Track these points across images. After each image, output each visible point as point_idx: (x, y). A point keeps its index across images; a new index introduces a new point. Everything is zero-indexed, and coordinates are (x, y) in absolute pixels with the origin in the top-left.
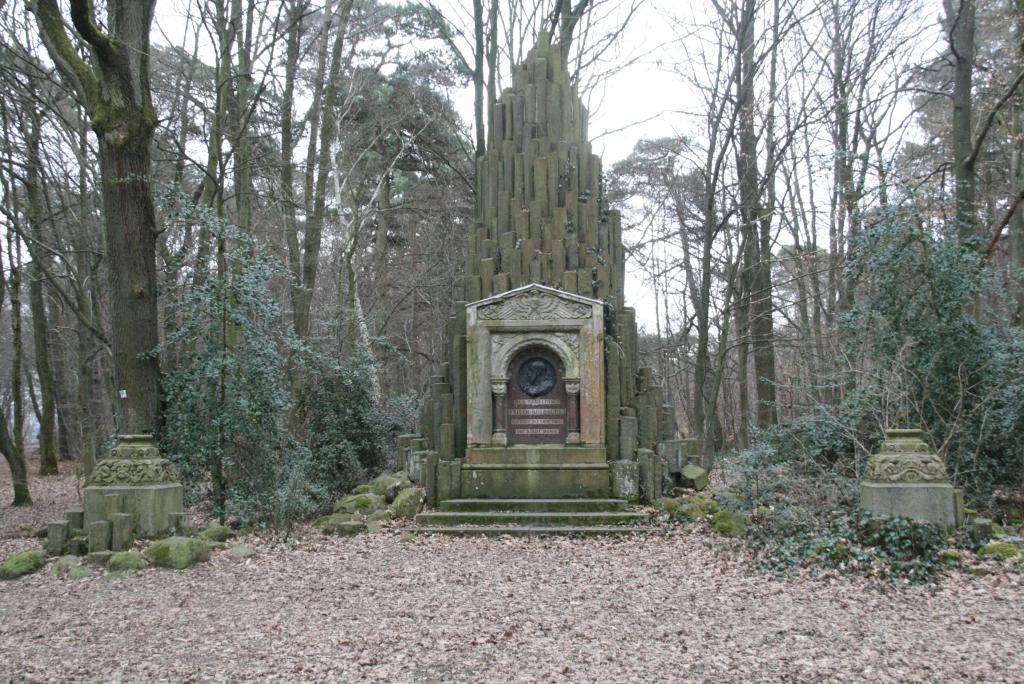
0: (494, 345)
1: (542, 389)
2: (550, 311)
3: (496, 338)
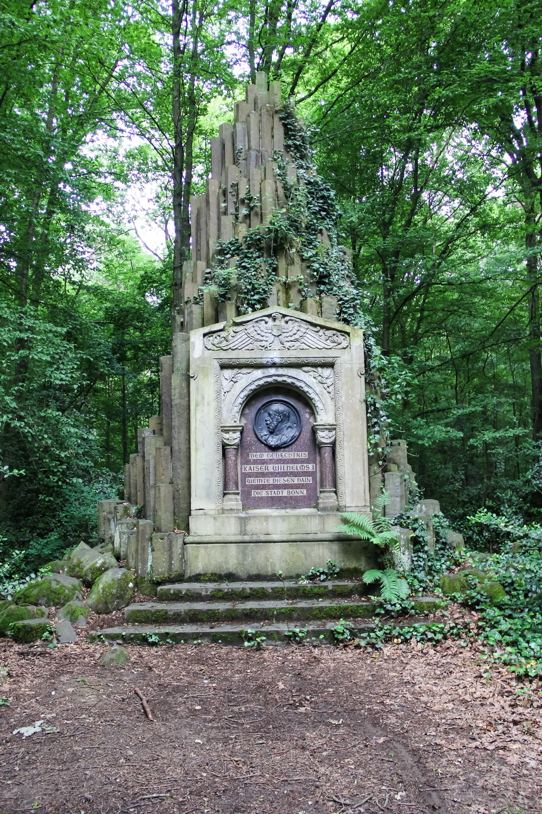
0: (225, 383)
1: (285, 439)
2: (297, 340)
3: (228, 373)
